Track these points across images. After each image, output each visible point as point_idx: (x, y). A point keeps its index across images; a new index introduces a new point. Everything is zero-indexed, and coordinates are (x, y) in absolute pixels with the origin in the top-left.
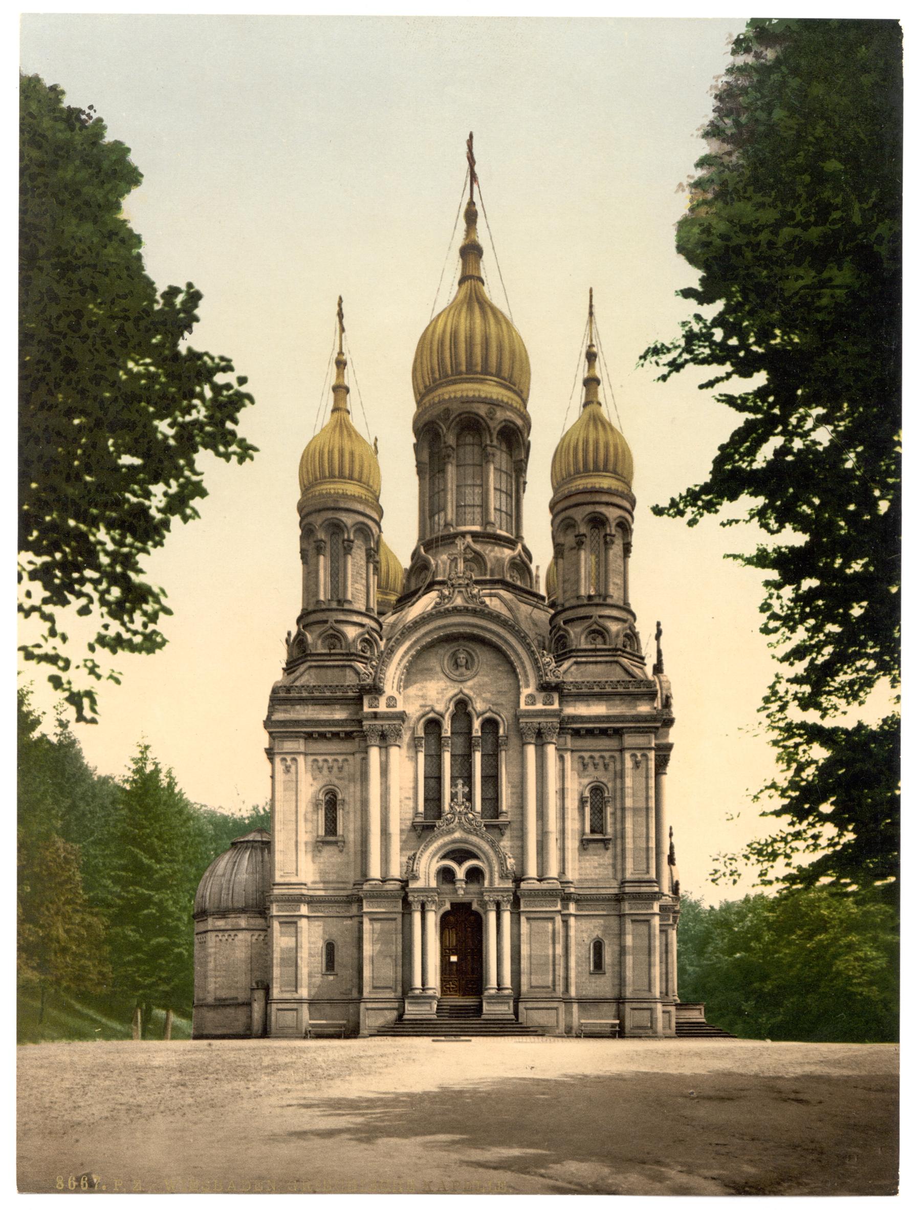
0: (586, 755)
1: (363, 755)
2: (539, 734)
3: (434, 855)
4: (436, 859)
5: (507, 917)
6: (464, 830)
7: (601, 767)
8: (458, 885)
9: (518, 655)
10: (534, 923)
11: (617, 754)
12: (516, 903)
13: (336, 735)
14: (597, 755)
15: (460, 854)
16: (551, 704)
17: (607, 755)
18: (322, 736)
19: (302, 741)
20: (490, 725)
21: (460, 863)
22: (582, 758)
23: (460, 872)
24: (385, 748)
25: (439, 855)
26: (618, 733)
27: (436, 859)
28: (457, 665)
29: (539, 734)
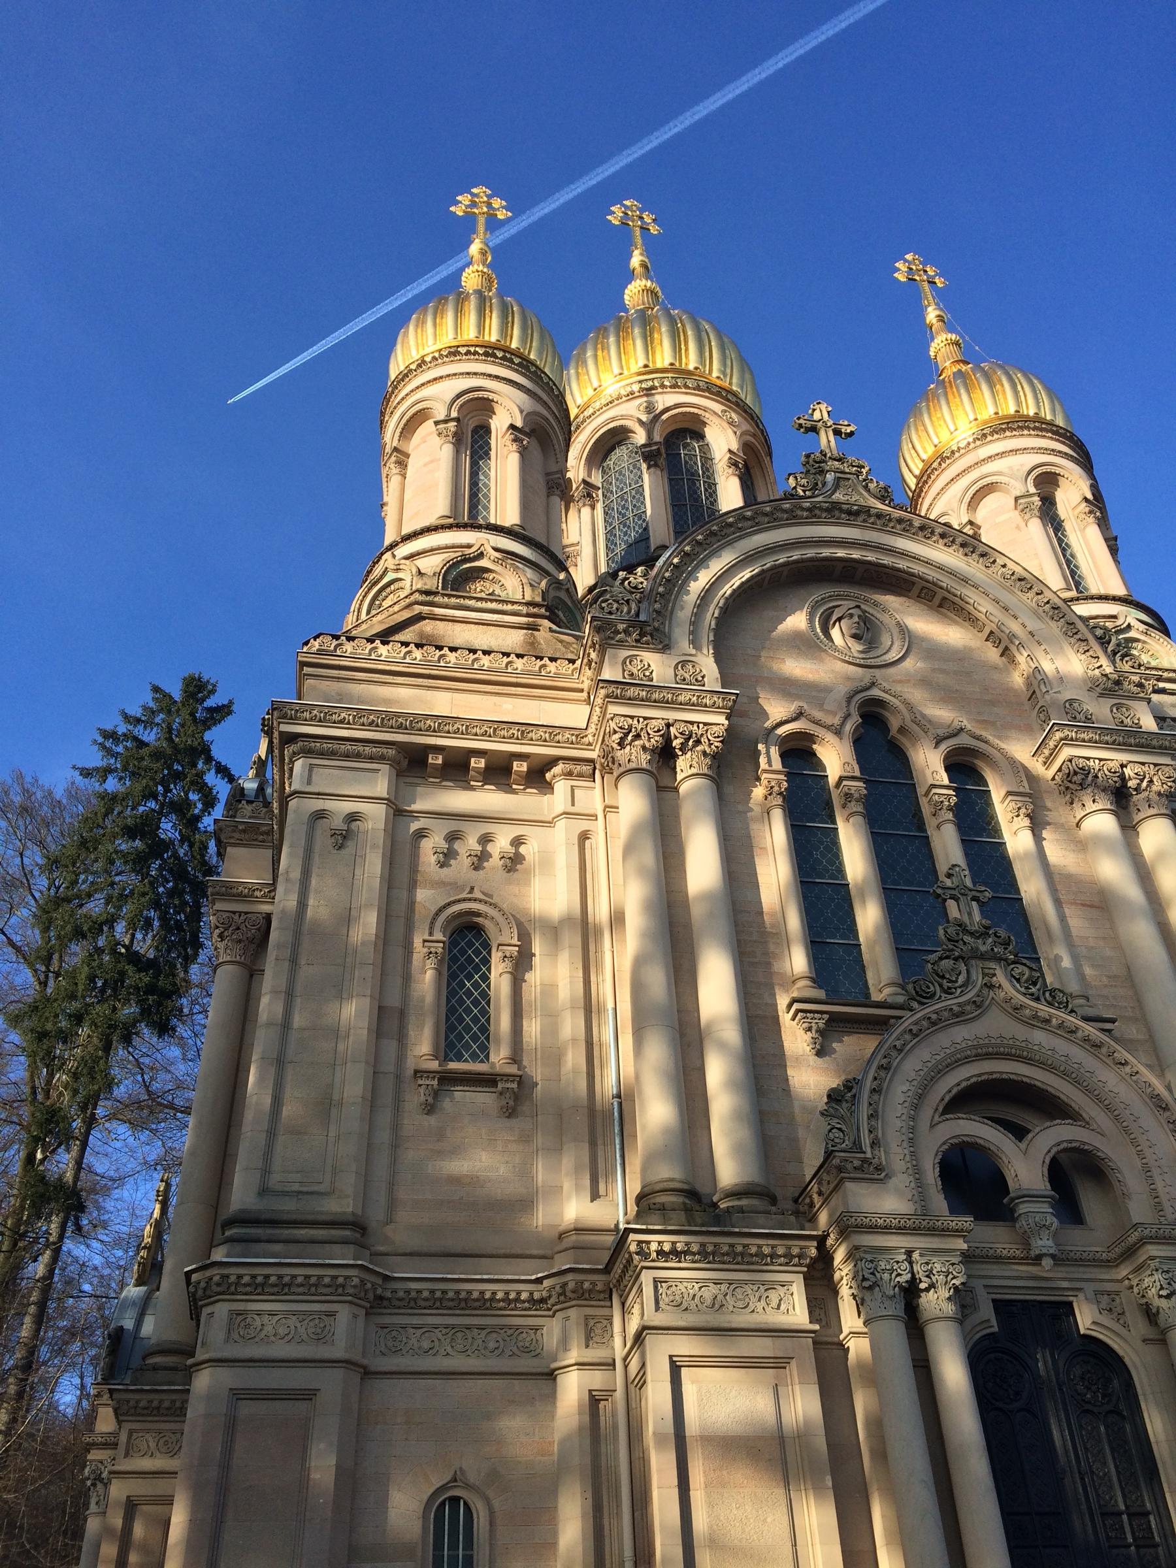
3: (920, 1097)
4: (927, 1113)
21: (1019, 1133)
27: (927, 1113)
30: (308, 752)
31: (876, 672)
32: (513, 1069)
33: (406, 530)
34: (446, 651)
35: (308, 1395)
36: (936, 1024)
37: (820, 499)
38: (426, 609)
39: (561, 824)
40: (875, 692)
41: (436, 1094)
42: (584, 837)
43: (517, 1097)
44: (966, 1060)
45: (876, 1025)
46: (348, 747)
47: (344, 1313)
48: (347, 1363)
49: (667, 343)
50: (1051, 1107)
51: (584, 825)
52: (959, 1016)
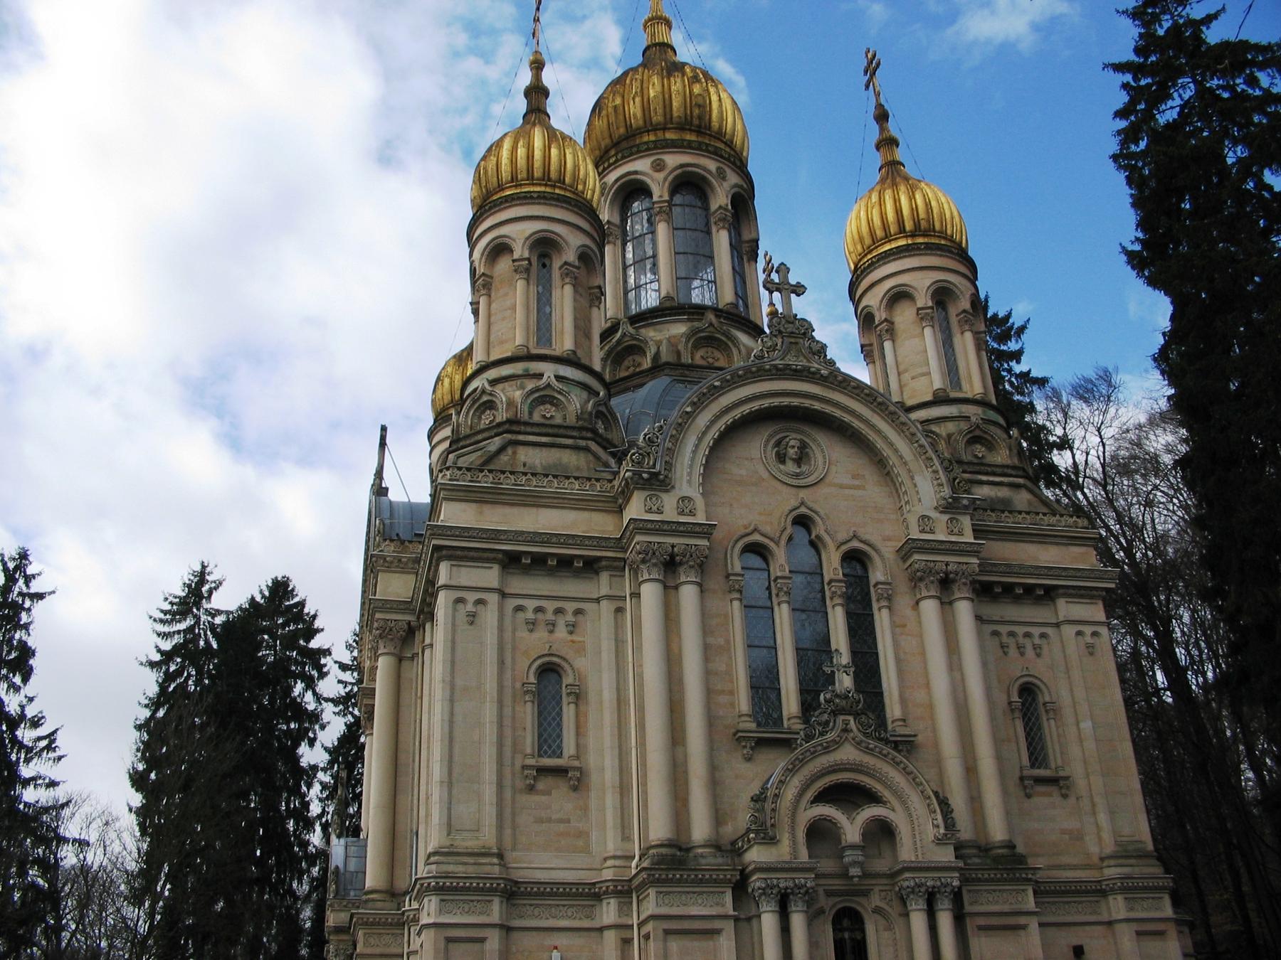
0: (1003, 629)
1: (620, 604)
2: (946, 583)
5: (945, 922)
6: (858, 745)
7: (1030, 652)
8: (849, 856)
9: (891, 444)
10: (1051, 932)
11: (1049, 631)
12: (957, 897)
13: (565, 564)
14: (1020, 630)
15: (849, 794)
16: (961, 534)
17: (1036, 631)
18: (539, 562)
19: (496, 568)
20: (856, 559)
22: (995, 634)
23: (851, 828)
24: (670, 589)
25: (809, 795)
26: (1049, 595)
28: (781, 458)
29: (946, 583)
30: (449, 558)
31: (803, 494)
32: (576, 763)
33: (493, 357)
34: (529, 476)
35: (482, 940)
36: (814, 754)
37: (777, 362)
38: (513, 437)
39: (604, 603)
40: (803, 510)
41: (535, 778)
42: (620, 610)
43: (579, 780)
44: (829, 773)
45: (785, 744)
46: (472, 554)
47: (496, 901)
48: (501, 926)
49: (674, 109)
50: (872, 798)
51: (620, 604)
52: (827, 749)
